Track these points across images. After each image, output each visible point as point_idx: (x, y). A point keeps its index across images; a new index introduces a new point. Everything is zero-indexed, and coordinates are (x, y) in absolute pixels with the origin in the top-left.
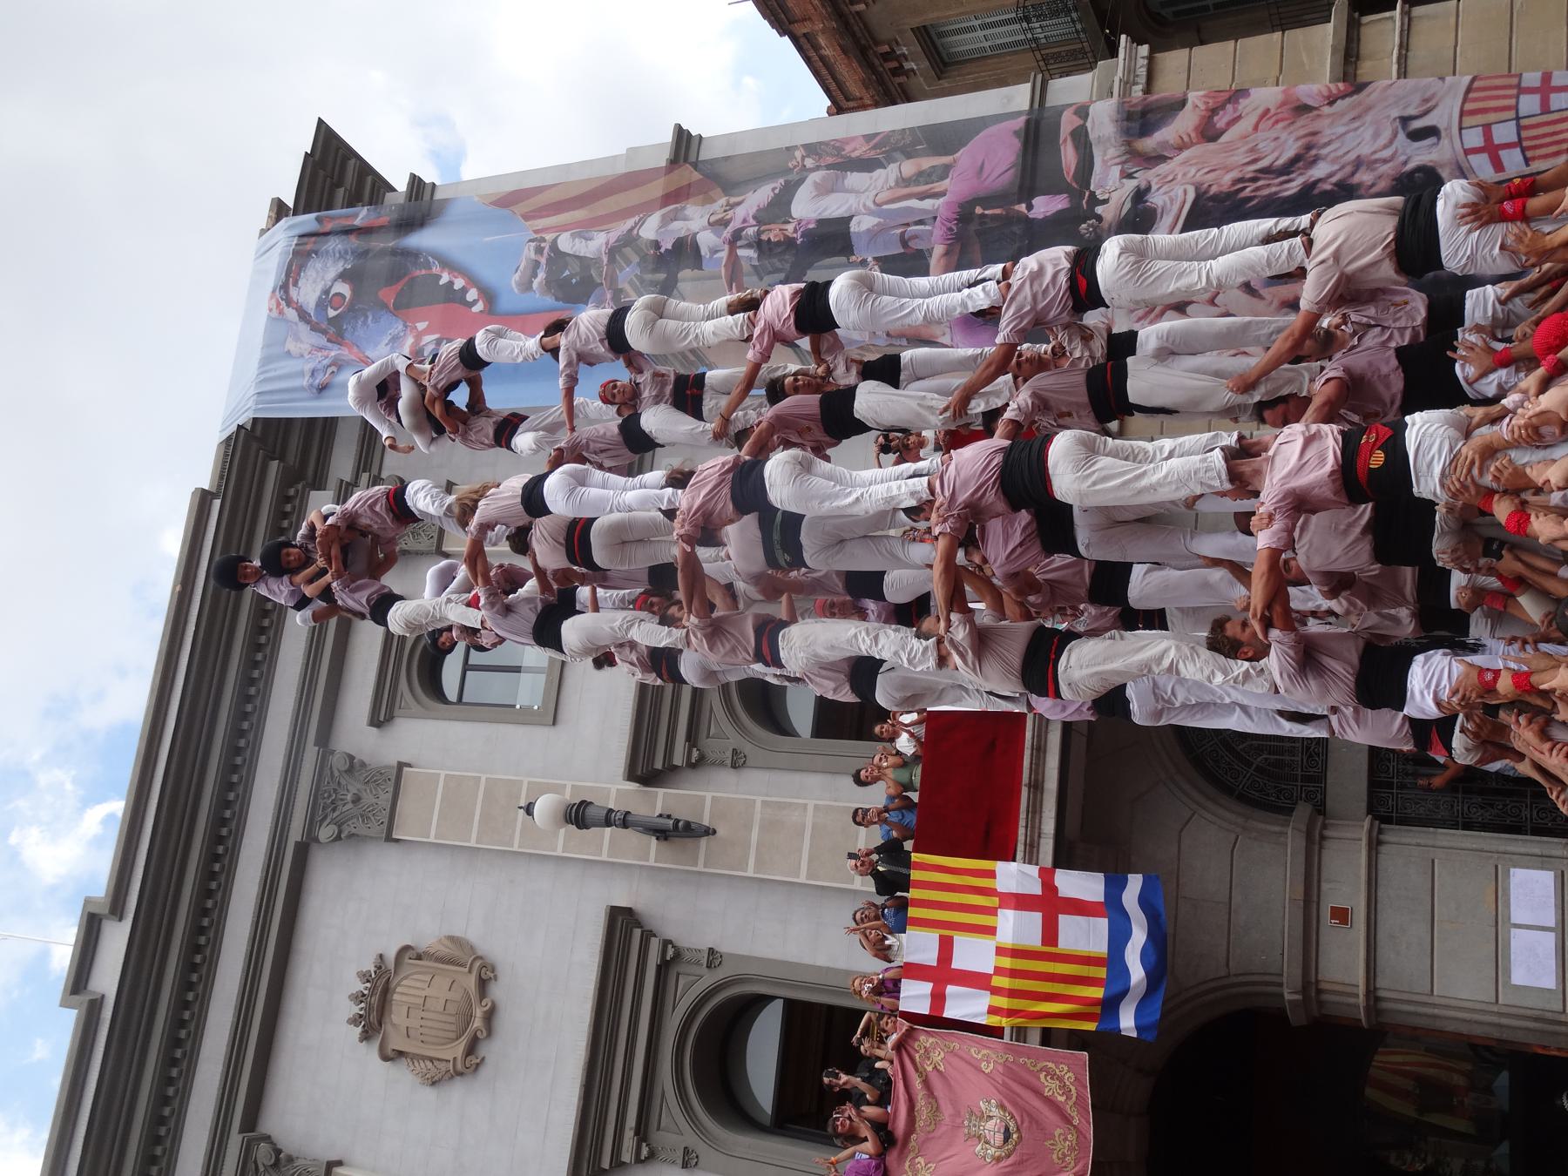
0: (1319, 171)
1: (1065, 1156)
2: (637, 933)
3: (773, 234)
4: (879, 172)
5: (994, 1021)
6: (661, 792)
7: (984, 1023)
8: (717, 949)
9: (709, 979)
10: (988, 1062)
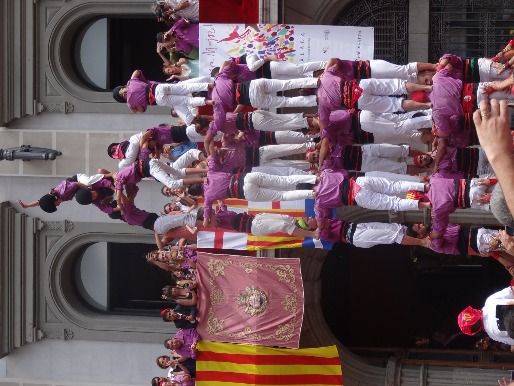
1: (291, 307)
2: (18, 216)
5: (251, 248)
6: (21, 132)
7: (245, 249)
8: (69, 220)
9: (66, 238)
10: (249, 268)
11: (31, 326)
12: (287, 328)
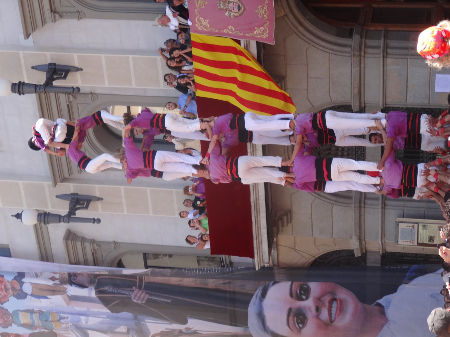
11: (49, 11)
12: (262, 30)
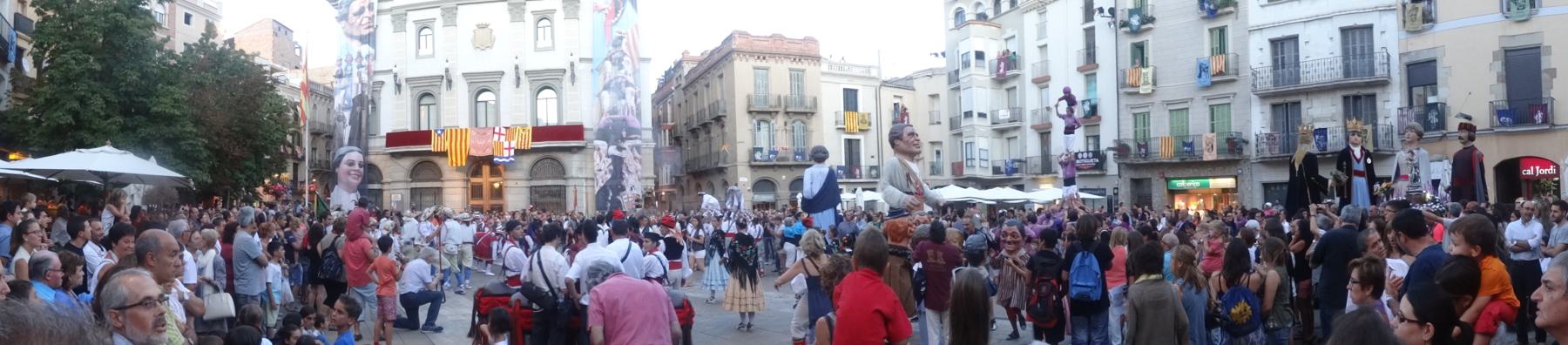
0: (627, 175)
3: (623, 84)
4: (633, 102)
